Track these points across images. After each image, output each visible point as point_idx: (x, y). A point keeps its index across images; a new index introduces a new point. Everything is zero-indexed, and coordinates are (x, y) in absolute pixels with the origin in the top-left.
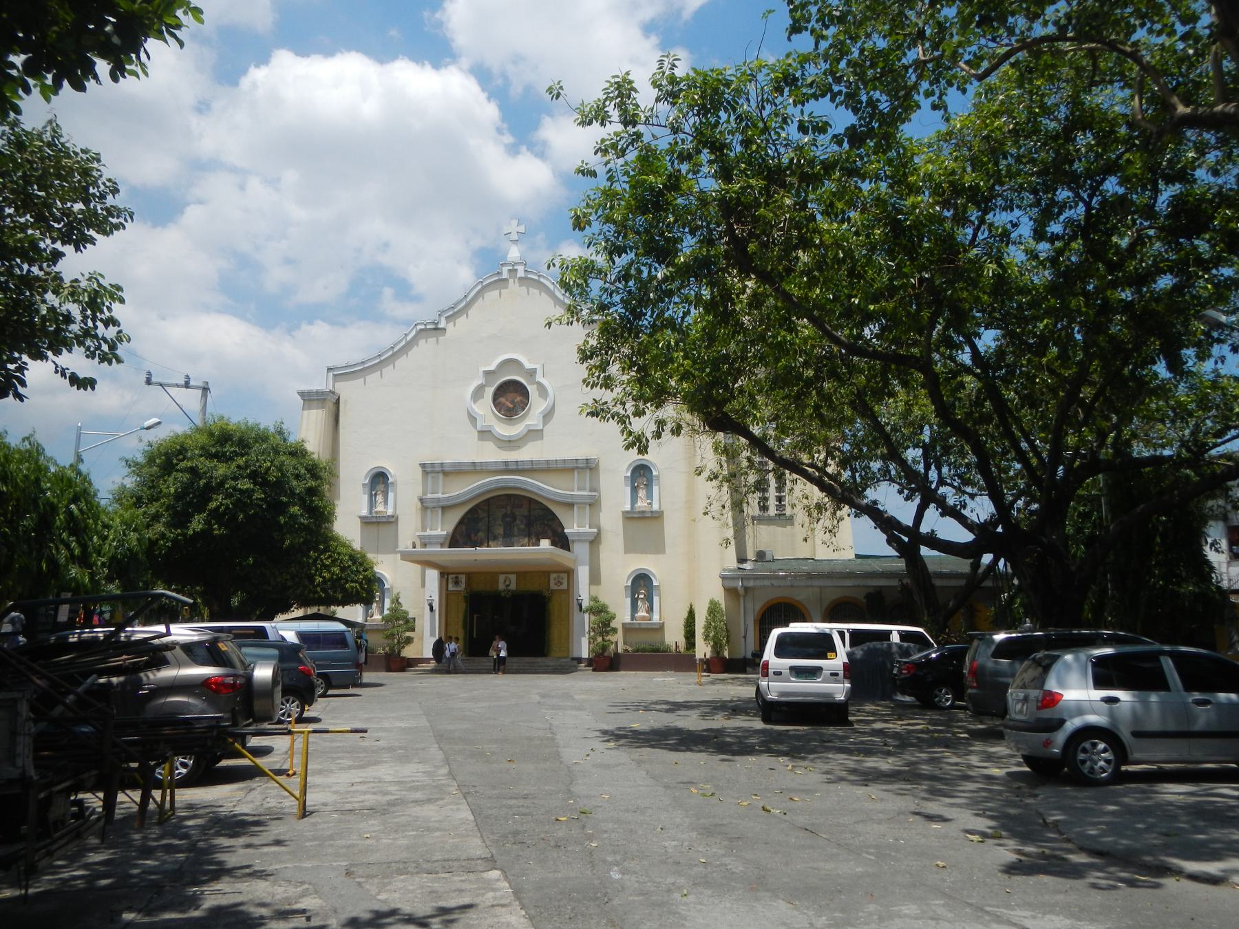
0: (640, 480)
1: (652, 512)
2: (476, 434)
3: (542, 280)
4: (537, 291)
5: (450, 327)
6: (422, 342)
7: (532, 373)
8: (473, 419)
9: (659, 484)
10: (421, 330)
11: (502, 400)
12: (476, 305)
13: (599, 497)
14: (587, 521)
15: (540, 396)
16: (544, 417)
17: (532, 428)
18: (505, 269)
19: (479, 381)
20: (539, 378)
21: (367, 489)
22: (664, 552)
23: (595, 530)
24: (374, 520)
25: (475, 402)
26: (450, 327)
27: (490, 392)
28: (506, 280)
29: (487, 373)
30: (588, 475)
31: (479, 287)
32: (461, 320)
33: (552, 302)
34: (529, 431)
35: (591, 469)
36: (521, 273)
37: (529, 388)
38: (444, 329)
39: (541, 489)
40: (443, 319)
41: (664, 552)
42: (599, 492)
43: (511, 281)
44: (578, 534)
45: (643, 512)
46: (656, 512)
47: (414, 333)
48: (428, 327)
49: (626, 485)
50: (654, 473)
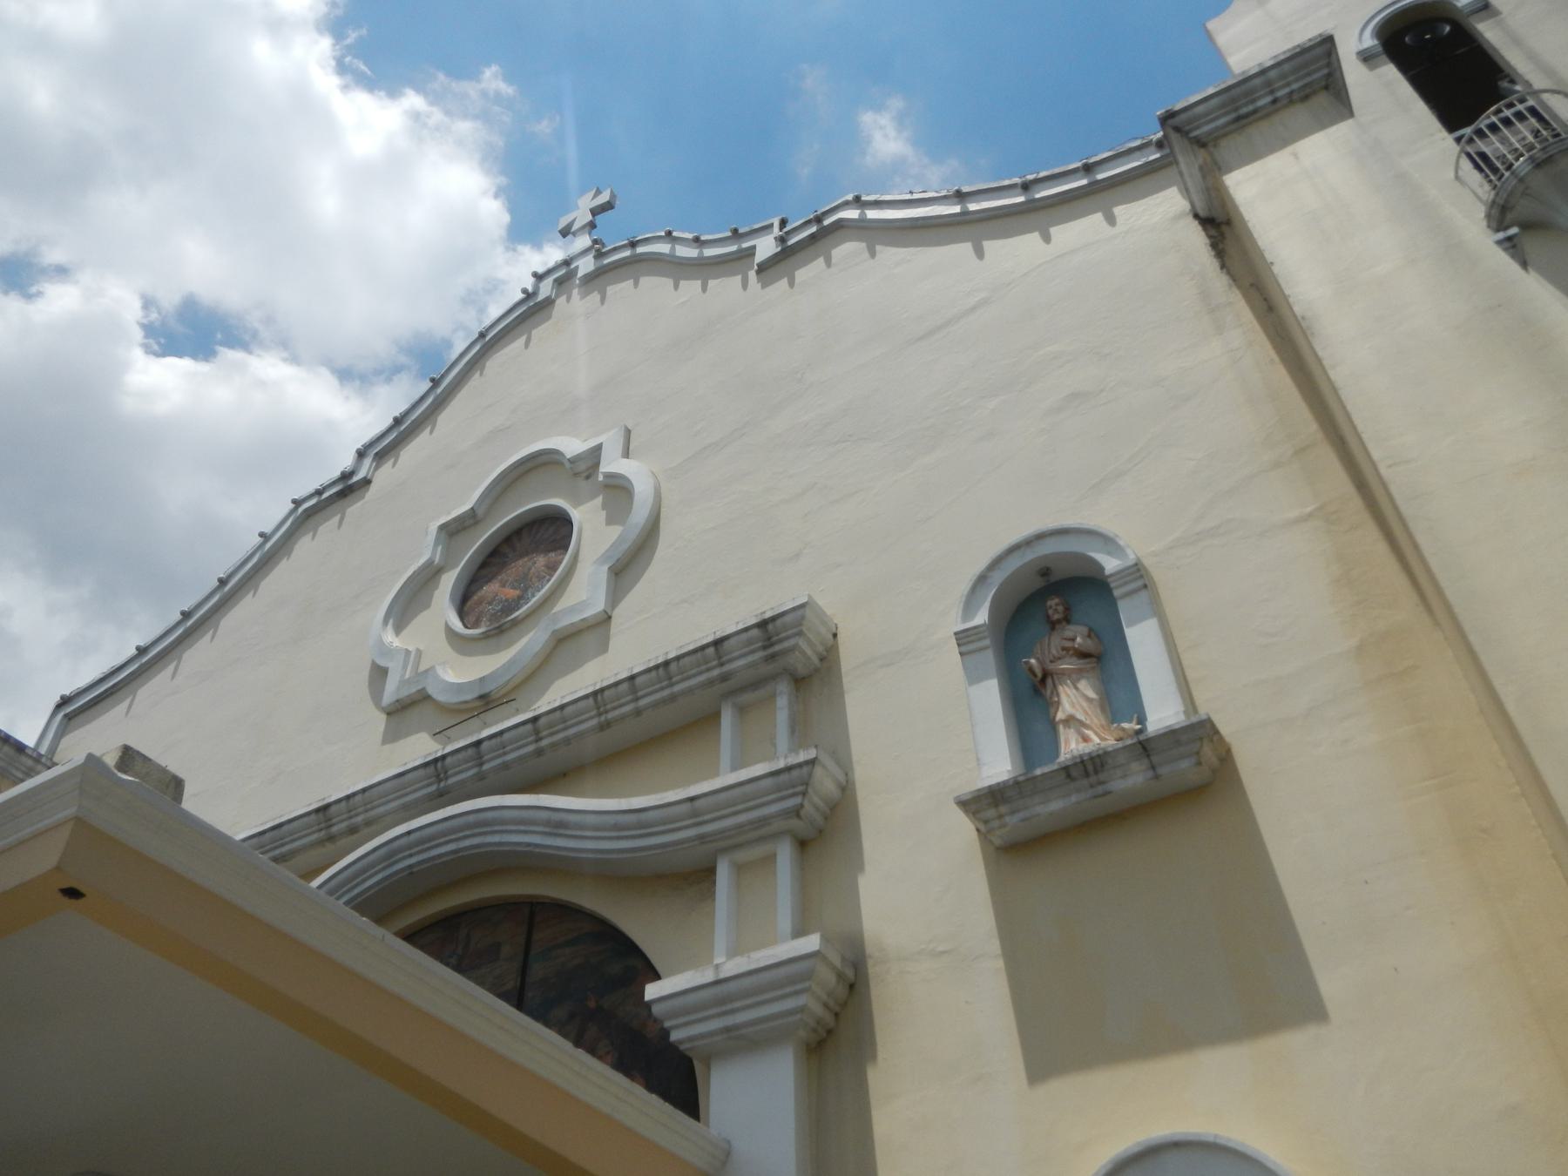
0: (1055, 643)
1: (1145, 747)
2: (383, 717)
3: (640, 250)
4: (631, 282)
6: (305, 546)
9: (1156, 609)
11: (490, 589)
12: (466, 387)
13: (847, 788)
14: (784, 919)
15: (610, 521)
18: (546, 288)
19: (425, 550)
20: (612, 464)
22: (1309, 1009)
23: (811, 943)
25: (398, 630)
26: (385, 476)
27: (449, 581)
28: (549, 303)
29: (454, 530)
30: (782, 702)
31: (477, 348)
33: (669, 282)
35: (800, 682)
36: (586, 265)
37: (576, 514)
38: (366, 482)
39: (558, 823)
40: (367, 462)
41: (1309, 1009)
42: (847, 769)
43: (561, 301)
44: (722, 994)
45: (1092, 766)
46: (1172, 736)
48: (325, 495)
49: (973, 678)
50: (1110, 564)
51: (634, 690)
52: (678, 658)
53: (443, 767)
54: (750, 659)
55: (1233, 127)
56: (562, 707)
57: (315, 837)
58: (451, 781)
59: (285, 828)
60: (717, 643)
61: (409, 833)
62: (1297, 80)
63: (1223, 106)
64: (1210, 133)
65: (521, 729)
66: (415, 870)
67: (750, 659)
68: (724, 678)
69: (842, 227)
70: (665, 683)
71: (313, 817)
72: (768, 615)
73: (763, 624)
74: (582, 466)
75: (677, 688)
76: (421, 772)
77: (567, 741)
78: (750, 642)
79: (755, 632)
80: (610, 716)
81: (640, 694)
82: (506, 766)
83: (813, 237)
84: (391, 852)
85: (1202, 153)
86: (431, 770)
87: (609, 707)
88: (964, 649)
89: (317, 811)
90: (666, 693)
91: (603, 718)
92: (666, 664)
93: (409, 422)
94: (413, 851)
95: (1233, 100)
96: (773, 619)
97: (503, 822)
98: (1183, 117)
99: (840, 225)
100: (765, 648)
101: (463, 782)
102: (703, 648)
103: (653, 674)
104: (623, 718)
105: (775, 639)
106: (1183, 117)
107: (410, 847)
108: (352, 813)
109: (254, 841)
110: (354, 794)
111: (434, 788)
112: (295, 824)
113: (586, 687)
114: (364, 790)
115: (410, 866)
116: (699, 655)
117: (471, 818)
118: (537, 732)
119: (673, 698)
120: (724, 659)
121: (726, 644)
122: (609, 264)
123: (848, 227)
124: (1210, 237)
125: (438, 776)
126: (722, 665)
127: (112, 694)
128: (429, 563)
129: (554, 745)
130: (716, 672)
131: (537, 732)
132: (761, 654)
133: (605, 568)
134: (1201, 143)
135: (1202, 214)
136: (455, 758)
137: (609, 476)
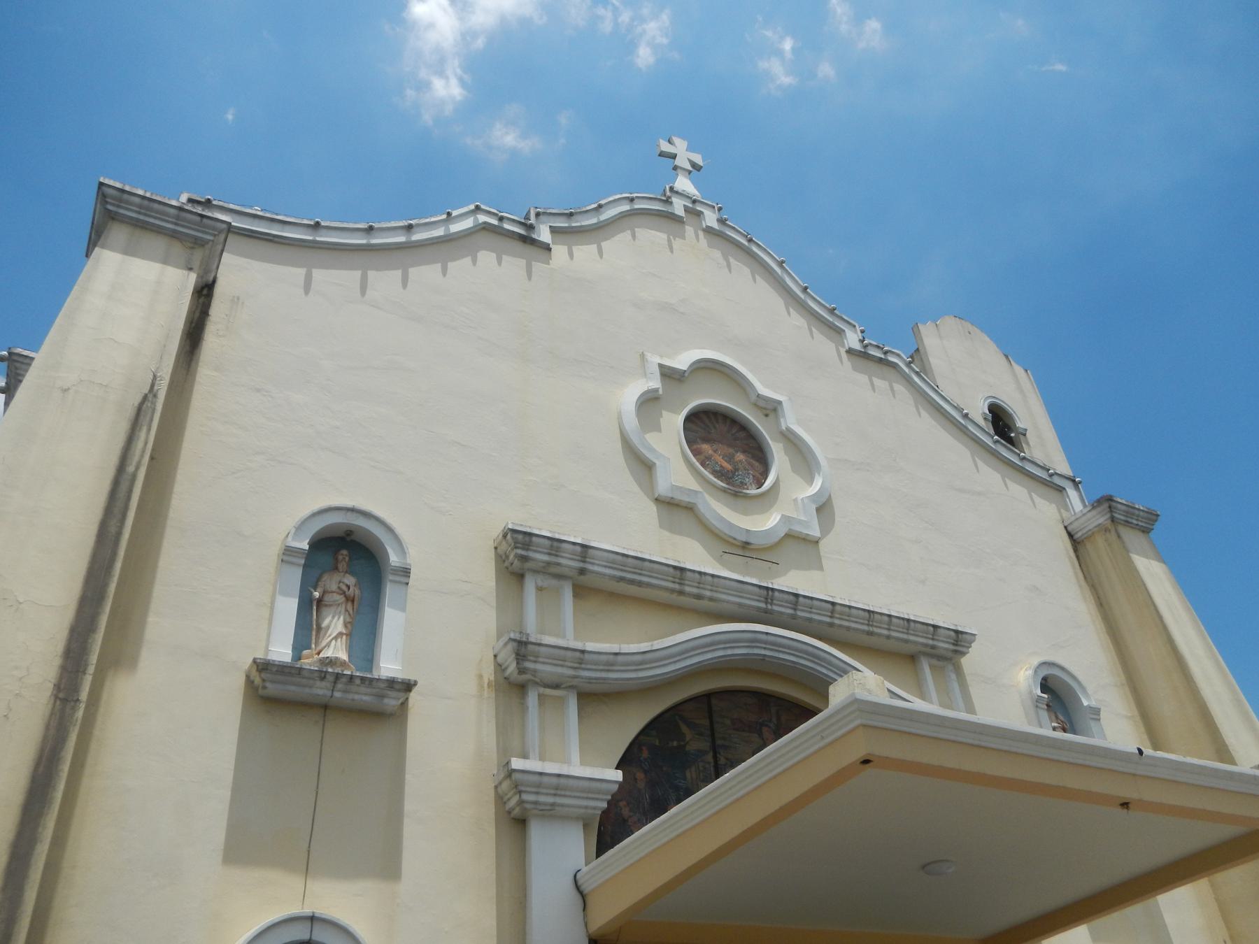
5: (559, 251)
7: (771, 409)
8: (643, 466)
10: (486, 227)
16: (819, 510)
17: (798, 528)
21: (296, 575)
24: (321, 690)
26: (559, 251)
29: (668, 374)
31: (625, 207)
32: (585, 252)
34: (790, 536)
38: (547, 248)
43: (689, 230)
47: (468, 223)
51: (890, 623)
52: (914, 621)
53: (772, 596)
54: (946, 646)
55: (1122, 522)
56: (850, 607)
57: (671, 585)
58: (775, 608)
59: (647, 564)
60: (935, 627)
61: (767, 633)
62: (1146, 523)
63: (1124, 511)
64: (1118, 519)
65: (824, 604)
66: (767, 659)
67: (946, 646)
68: (933, 647)
69: (894, 367)
70: (905, 631)
71: (671, 570)
72: (960, 629)
73: (957, 632)
74: (762, 403)
75: (912, 638)
76: (757, 590)
77: (848, 628)
78: (949, 637)
79: (952, 634)
80: (876, 630)
81: (892, 628)
82: (810, 620)
83: (880, 360)
84: (754, 639)
85: (1109, 521)
86: (765, 592)
87: (875, 624)
88: (1039, 705)
89: (675, 568)
90: (905, 636)
91: (871, 629)
92: (908, 620)
93: (578, 224)
94: (768, 646)
95: (1127, 512)
96: (962, 633)
97: (830, 663)
98: (1114, 504)
99: (894, 366)
100: (954, 644)
101: (782, 613)
102: (927, 625)
103: (901, 622)
104: (879, 635)
105: (959, 643)
106: (1114, 504)
107: (766, 643)
108: (701, 586)
109: (620, 558)
110: (705, 574)
111: (763, 605)
112: (656, 566)
113: (864, 604)
114: (713, 576)
115: (765, 655)
116: (925, 627)
117: (811, 649)
118: (833, 612)
119: (906, 641)
120: (935, 637)
121: (938, 630)
122: (728, 235)
123: (898, 371)
124: (1072, 545)
125: (766, 599)
126: (933, 639)
127: (271, 241)
128: (656, 390)
129: (840, 626)
130: (931, 642)
131: (833, 612)
132: (952, 647)
133: (814, 507)
134: (1113, 519)
135: (1069, 529)
136: (781, 595)
137: (788, 429)
